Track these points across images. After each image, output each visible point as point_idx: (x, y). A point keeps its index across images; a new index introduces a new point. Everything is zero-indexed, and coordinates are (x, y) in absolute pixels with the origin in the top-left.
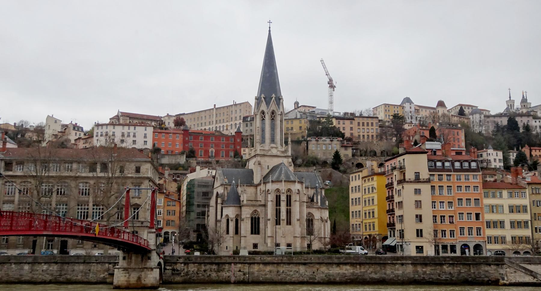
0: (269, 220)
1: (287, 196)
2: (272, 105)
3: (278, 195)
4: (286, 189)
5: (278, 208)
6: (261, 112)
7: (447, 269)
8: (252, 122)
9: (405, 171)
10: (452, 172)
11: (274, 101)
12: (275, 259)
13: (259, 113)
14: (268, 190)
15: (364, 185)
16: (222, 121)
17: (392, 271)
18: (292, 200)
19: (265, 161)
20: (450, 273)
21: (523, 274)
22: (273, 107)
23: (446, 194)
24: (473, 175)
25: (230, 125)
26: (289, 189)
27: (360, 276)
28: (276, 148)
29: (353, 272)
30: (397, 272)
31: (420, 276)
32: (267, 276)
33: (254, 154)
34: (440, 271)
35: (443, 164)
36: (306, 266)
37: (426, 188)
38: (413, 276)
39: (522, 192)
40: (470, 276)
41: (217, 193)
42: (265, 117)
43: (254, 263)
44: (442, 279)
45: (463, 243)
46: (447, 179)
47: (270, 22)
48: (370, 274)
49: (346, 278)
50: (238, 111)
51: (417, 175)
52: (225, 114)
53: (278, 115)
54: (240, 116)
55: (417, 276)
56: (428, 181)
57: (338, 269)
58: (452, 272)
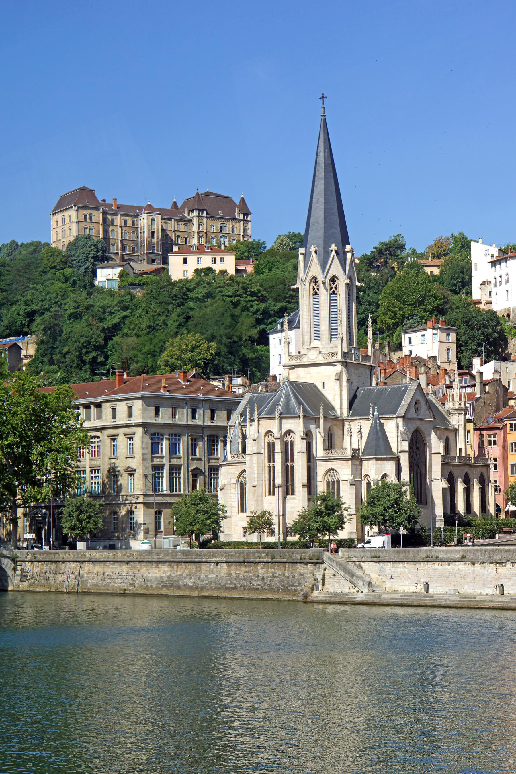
7: (260, 570)
20: (263, 578)
27: (176, 581)
29: (170, 575)
30: (211, 576)
31: (232, 583)
32: (94, 581)
34: (254, 575)
36: (129, 566)
38: (225, 582)
40: (282, 583)
43: (85, 562)
44: (254, 587)
48: (185, 578)
49: (162, 584)
57: (156, 571)
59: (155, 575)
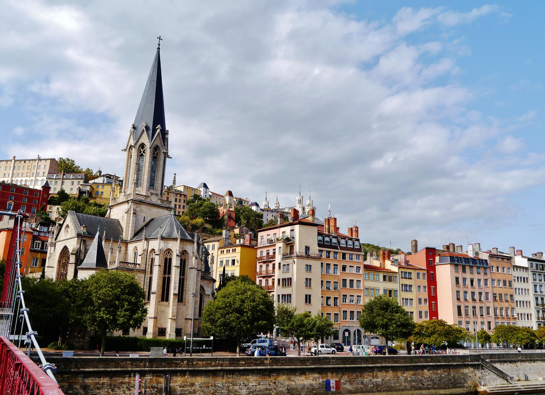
0: (154, 293)
1: (181, 260)
2: (156, 138)
3: (168, 257)
4: (181, 250)
5: (167, 276)
6: (140, 145)
8: (56, 180)
9: (294, 243)
10: (338, 249)
11: (159, 134)
12: (211, 364)
13: (137, 146)
14: (153, 250)
15: (219, 257)
16: (20, 175)
17: (370, 378)
18: (186, 266)
19: (142, 211)
21: (495, 376)
22: (159, 142)
23: (332, 273)
24: (357, 255)
25: (30, 180)
26: (185, 251)
28: (157, 195)
31: (401, 385)
33: (125, 200)
35: (331, 240)
37: (316, 265)
39: (394, 276)
41: (65, 248)
42: (144, 152)
45: (345, 328)
46: (334, 257)
47: (160, 39)
48: (345, 384)
50: (42, 167)
51: (307, 248)
52: (26, 168)
53: (162, 154)
54: (44, 173)
55: (397, 385)
56: (319, 258)
57: (303, 378)
58: (434, 377)
59: (302, 382)
